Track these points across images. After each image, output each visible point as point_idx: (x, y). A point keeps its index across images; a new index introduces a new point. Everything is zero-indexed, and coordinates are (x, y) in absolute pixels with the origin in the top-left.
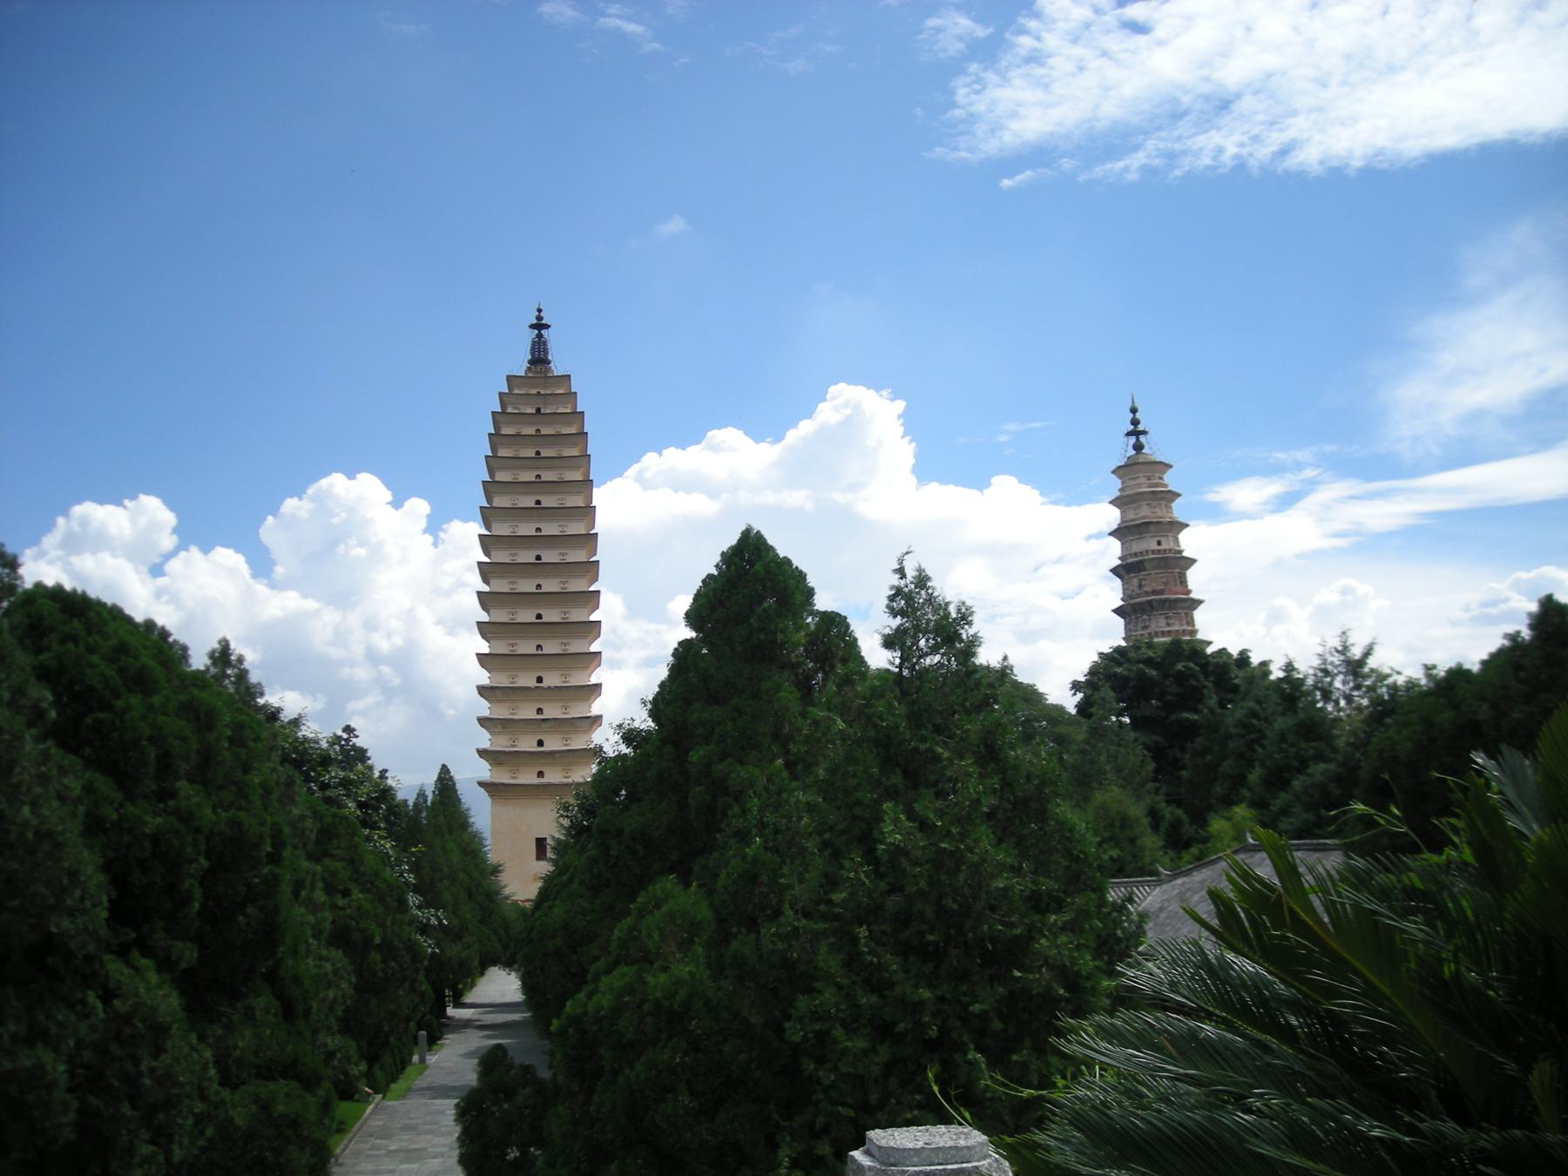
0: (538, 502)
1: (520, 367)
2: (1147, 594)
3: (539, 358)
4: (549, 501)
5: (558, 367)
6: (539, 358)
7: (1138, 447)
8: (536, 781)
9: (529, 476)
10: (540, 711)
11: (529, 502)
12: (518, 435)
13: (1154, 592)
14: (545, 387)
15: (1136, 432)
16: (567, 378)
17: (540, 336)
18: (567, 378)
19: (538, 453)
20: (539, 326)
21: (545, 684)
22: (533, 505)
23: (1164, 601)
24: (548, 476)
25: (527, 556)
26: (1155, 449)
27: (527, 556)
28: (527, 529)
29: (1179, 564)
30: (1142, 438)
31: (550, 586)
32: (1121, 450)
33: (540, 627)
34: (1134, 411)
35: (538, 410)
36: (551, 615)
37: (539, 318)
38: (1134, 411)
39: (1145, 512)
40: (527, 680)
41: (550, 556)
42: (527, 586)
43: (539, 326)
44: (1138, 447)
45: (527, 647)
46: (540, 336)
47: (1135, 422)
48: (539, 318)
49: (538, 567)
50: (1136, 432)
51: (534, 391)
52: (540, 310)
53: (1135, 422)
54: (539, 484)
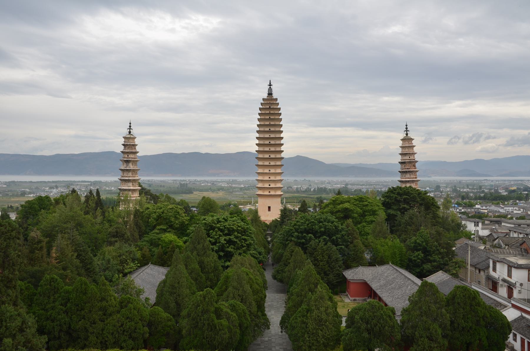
1: (265, 96)
3: (270, 94)
4: (272, 129)
5: (275, 96)
6: (270, 94)
7: (407, 134)
8: (268, 194)
9: (267, 123)
16: (276, 99)
18: (276, 99)
20: (270, 85)
23: (409, 172)
24: (272, 123)
25: (267, 142)
29: (413, 163)
31: (272, 149)
32: (403, 135)
34: (406, 126)
38: (406, 126)
39: (406, 151)
41: (272, 142)
42: (267, 149)
43: (270, 85)
44: (407, 134)
47: (407, 128)
49: (270, 145)
53: (407, 128)
54: (270, 125)
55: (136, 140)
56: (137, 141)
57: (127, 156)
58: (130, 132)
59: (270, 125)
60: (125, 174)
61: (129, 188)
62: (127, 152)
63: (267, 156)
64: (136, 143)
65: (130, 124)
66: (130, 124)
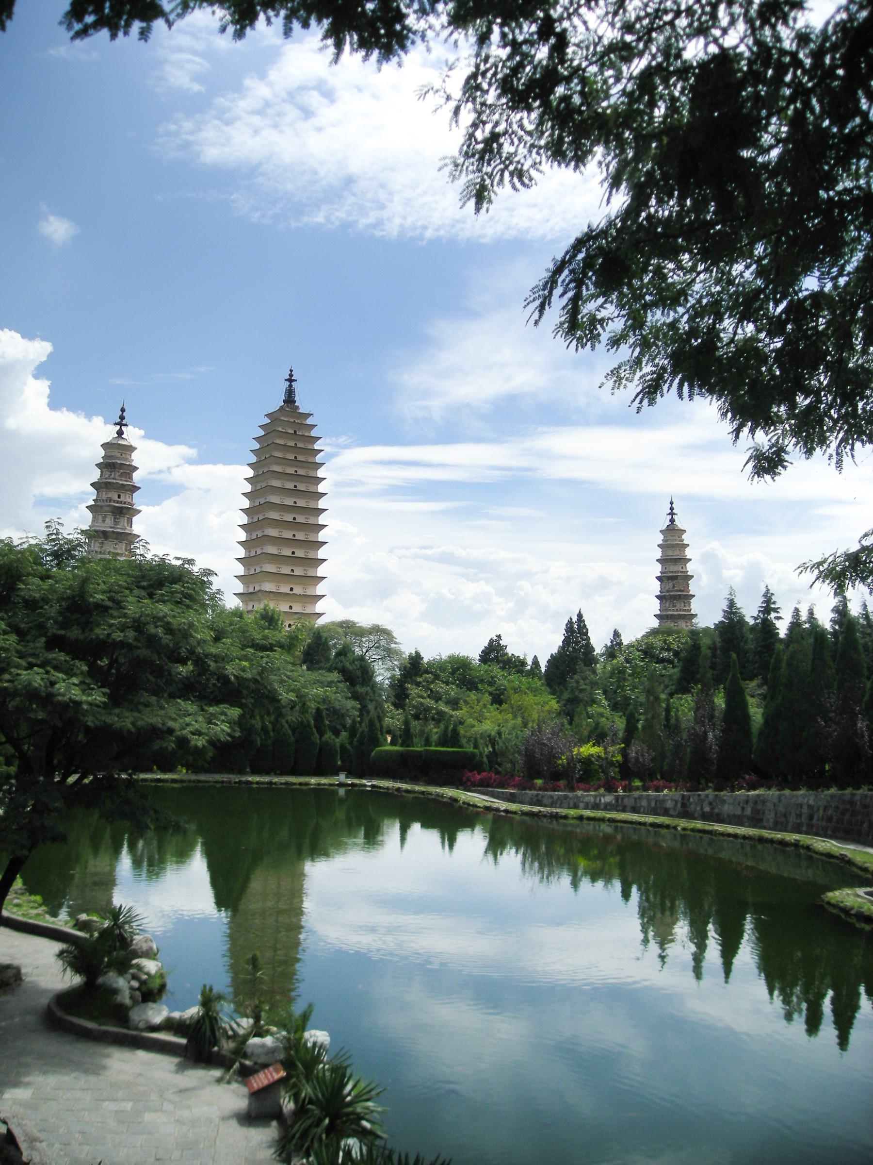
0: (295, 486)
2: (677, 591)
7: (672, 521)
9: (291, 471)
10: (291, 607)
11: (291, 486)
12: (285, 445)
13: (681, 591)
14: (298, 418)
15: (672, 514)
17: (290, 386)
18: (310, 415)
19: (296, 457)
20: (290, 380)
21: (295, 591)
22: (293, 488)
26: (680, 523)
27: (289, 517)
28: (289, 501)
30: (675, 517)
31: (300, 536)
34: (672, 503)
35: (295, 432)
37: (291, 375)
38: (672, 503)
40: (285, 589)
41: (300, 519)
42: (288, 534)
43: (290, 380)
44: (672, 521)
45: (286, 570)
46: (290, 386)
47: (672, 509)
48: (291, 375)
50: (672, 514)
51: (292, 420)
52: (291, 371)
53: (672, 509)
55: (134, 455)
57: (116, 498)
58: (120, 433)
59: (295, 476)
63: (287, 552)
64: (134, 464)
65: (123, 410)
66: (123, 410)
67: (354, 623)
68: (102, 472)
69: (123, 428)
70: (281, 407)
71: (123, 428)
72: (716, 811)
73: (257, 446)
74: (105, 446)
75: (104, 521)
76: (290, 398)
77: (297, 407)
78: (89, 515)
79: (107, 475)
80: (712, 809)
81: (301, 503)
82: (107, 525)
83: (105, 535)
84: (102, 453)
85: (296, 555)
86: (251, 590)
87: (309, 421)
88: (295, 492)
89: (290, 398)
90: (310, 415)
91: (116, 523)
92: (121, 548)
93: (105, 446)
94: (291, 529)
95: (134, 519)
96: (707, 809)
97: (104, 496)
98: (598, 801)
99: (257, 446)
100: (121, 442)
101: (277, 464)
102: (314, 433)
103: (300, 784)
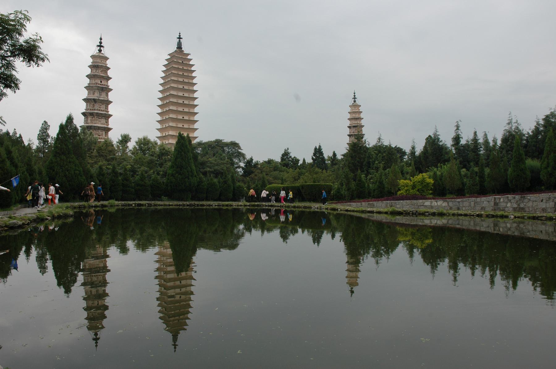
4: (186, 87)
9: (181, 80)
11: (181, 86)
12: (178, 68)
17: (180, 41)
18: (188, 54)
20: (180, 38)
24: (186, 80)
27: (180, 101)
28: (181, 94)
31: (186, 110)
33: (183, 121)
36: (186, 118)
37: (180, 36)
41: (186, 102)
42: (180, 109)
43: (180, 38)
46: (180, 41)
48: (180, 36)
54: (183, 83)
55: (108, 62)
56: (109, 63)
59: (183, 83)
60: (97, 106)
61: (103, 126)
62: (102, 77)
63: (180, 117)
65: (101, 39)
66: (101, 39)
67: (220, 141)
68: (92, 70)
69: (102, 48)
70: (176, 51)
71: (102, 48)
72: (522, 205)
73: (165, 69)
74: (93, 57)
75: (94, 94)
76: (179, 47)
77: (183, 51)
78: (86, 92)
79: (94, 71)
80: (519, 205)
81: (186, 95)
82: (96, 96)
83: (95, 101)
84: (91, 60)
85: (185, 118)
86: (164, 135)
87: (189, 57)
88: (183, 90)
89: (179, 47)
90: (188, 54)
91: (100, 95)
92: (103, 107)
93: (93, 57)
94: (182, 107)
95: (109, 93)
96: (515, 206)
97: (94, 82)
98: (433, 204)
99: (165, 69)
100: (101, 55)
101: (174, 76)
102: (191, 63)
103: (227, 205)
